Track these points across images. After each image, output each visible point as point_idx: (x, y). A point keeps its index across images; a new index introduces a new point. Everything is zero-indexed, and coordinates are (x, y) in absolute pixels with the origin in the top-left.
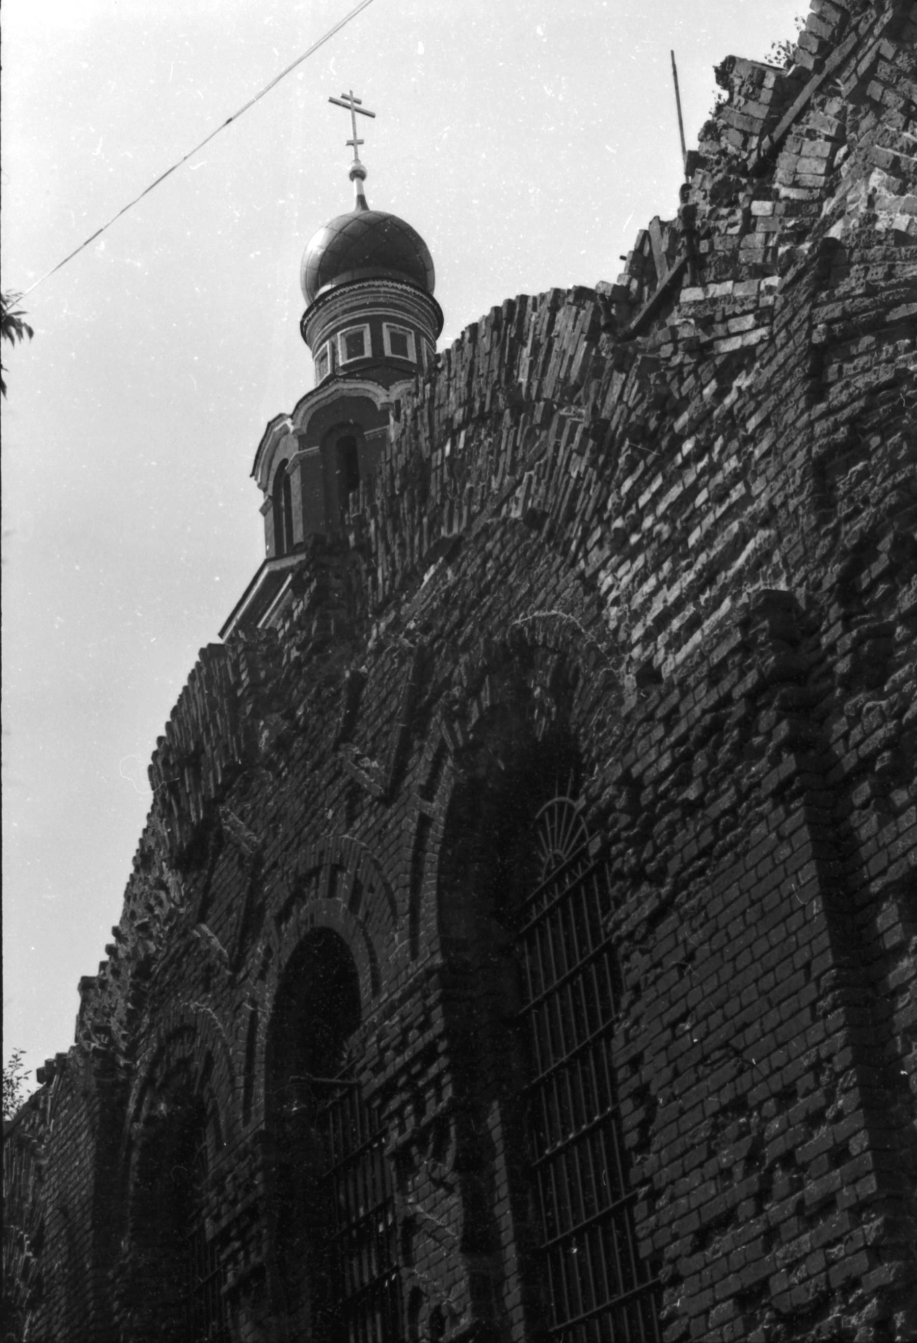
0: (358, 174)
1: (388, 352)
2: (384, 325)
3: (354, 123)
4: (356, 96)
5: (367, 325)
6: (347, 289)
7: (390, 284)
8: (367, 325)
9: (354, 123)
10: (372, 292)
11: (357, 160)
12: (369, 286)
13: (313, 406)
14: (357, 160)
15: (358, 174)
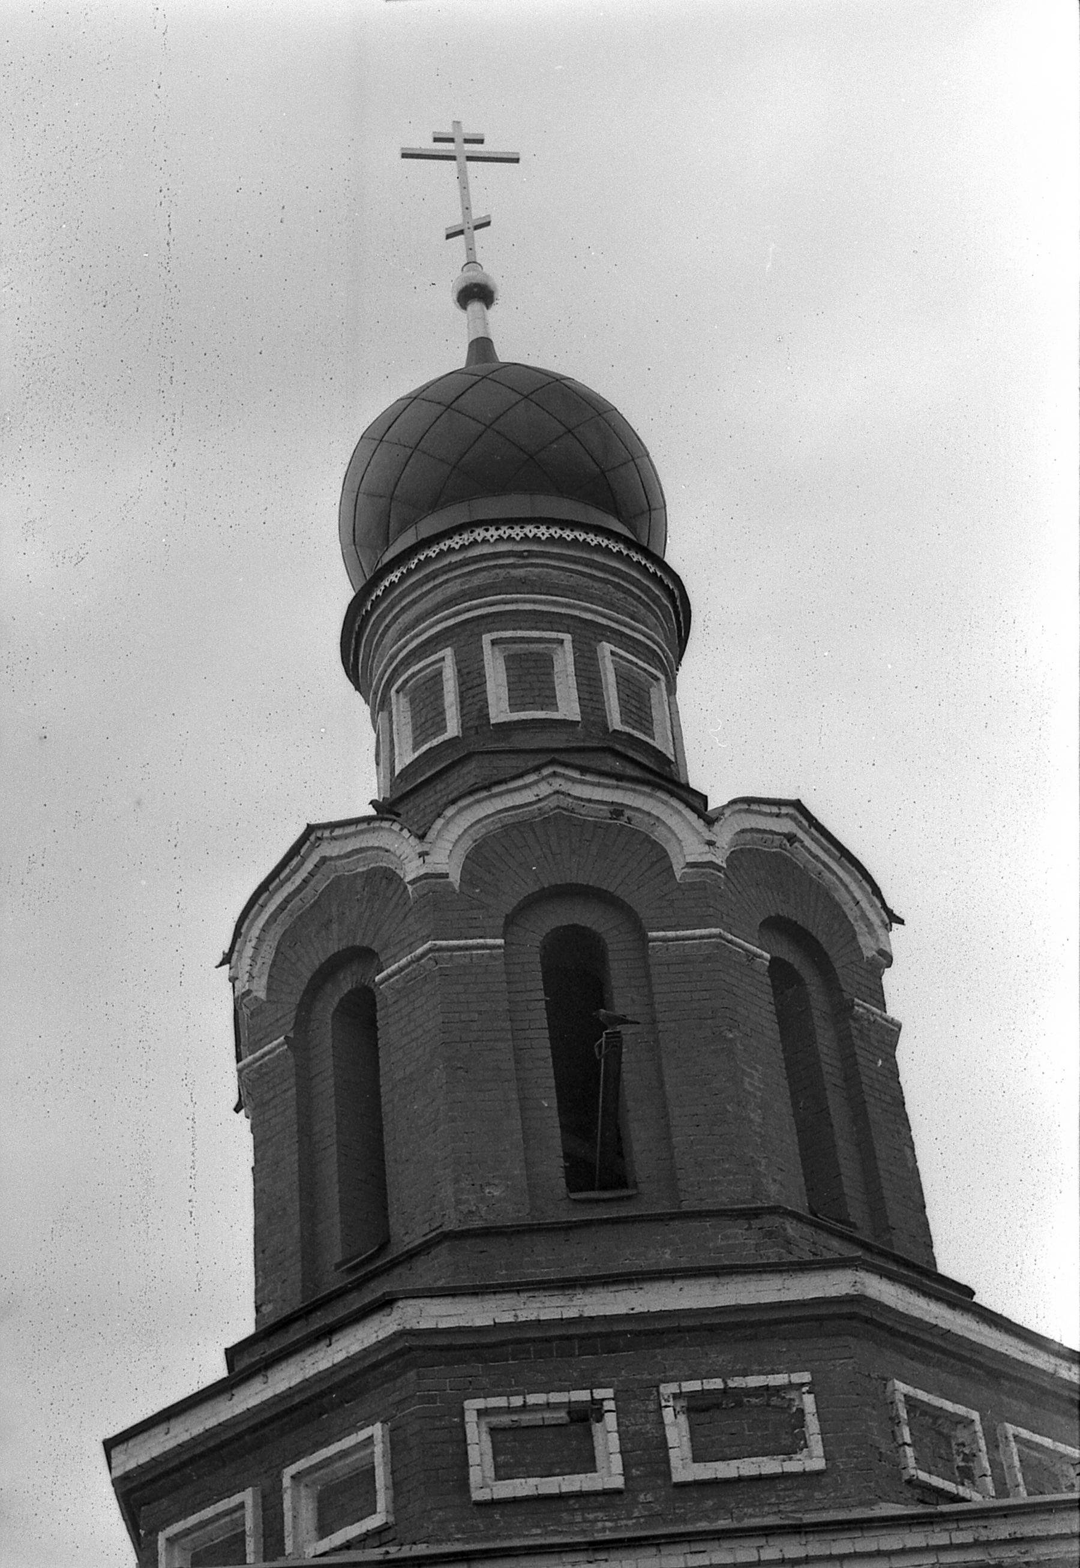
0: (476, 294)
1: (499, 711)
2: (487, 638)
3: (464, 187)
4: (470, 129)
5: (448, 652)
6: (394, 577)
7: (493, 533)
8: (448, 652)
9: (464, 187)
10: (452, 567)
11: (471, 262)
12: (441, 554)
13: (273, 917)
14: (471, 262)
15: (476, 294)
